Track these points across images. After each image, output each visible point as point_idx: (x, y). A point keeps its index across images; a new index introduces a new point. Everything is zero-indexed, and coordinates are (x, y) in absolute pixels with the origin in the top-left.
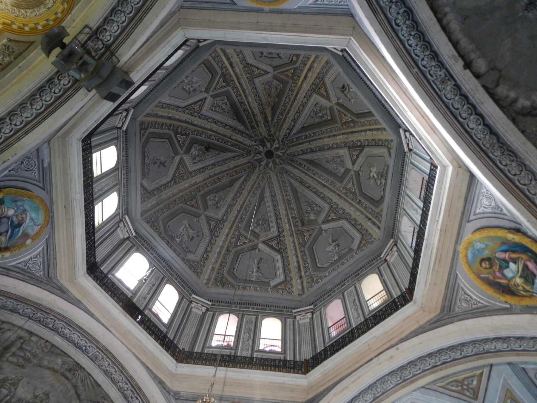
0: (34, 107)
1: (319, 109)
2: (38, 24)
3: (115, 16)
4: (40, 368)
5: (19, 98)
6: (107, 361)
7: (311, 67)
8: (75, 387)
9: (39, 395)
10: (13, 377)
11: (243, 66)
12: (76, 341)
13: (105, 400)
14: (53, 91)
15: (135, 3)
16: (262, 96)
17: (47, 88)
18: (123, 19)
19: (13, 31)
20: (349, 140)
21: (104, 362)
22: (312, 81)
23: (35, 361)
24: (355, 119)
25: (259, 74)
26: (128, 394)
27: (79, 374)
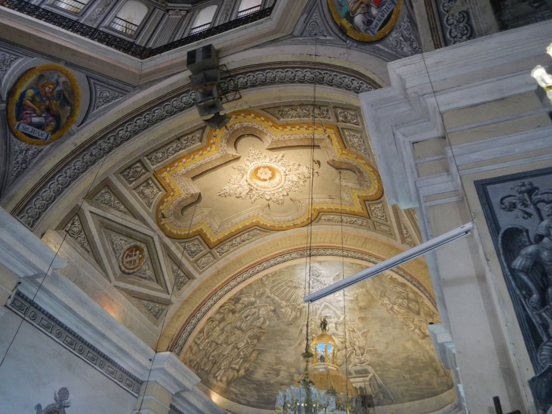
0: (273, 75)
2: (253, 118)
3: (182, 106)
5: (282, 87)
14: (254, 79)
15: (160, 110)
17: (258, 82)
18: (175, 102)
19: (273, 121)
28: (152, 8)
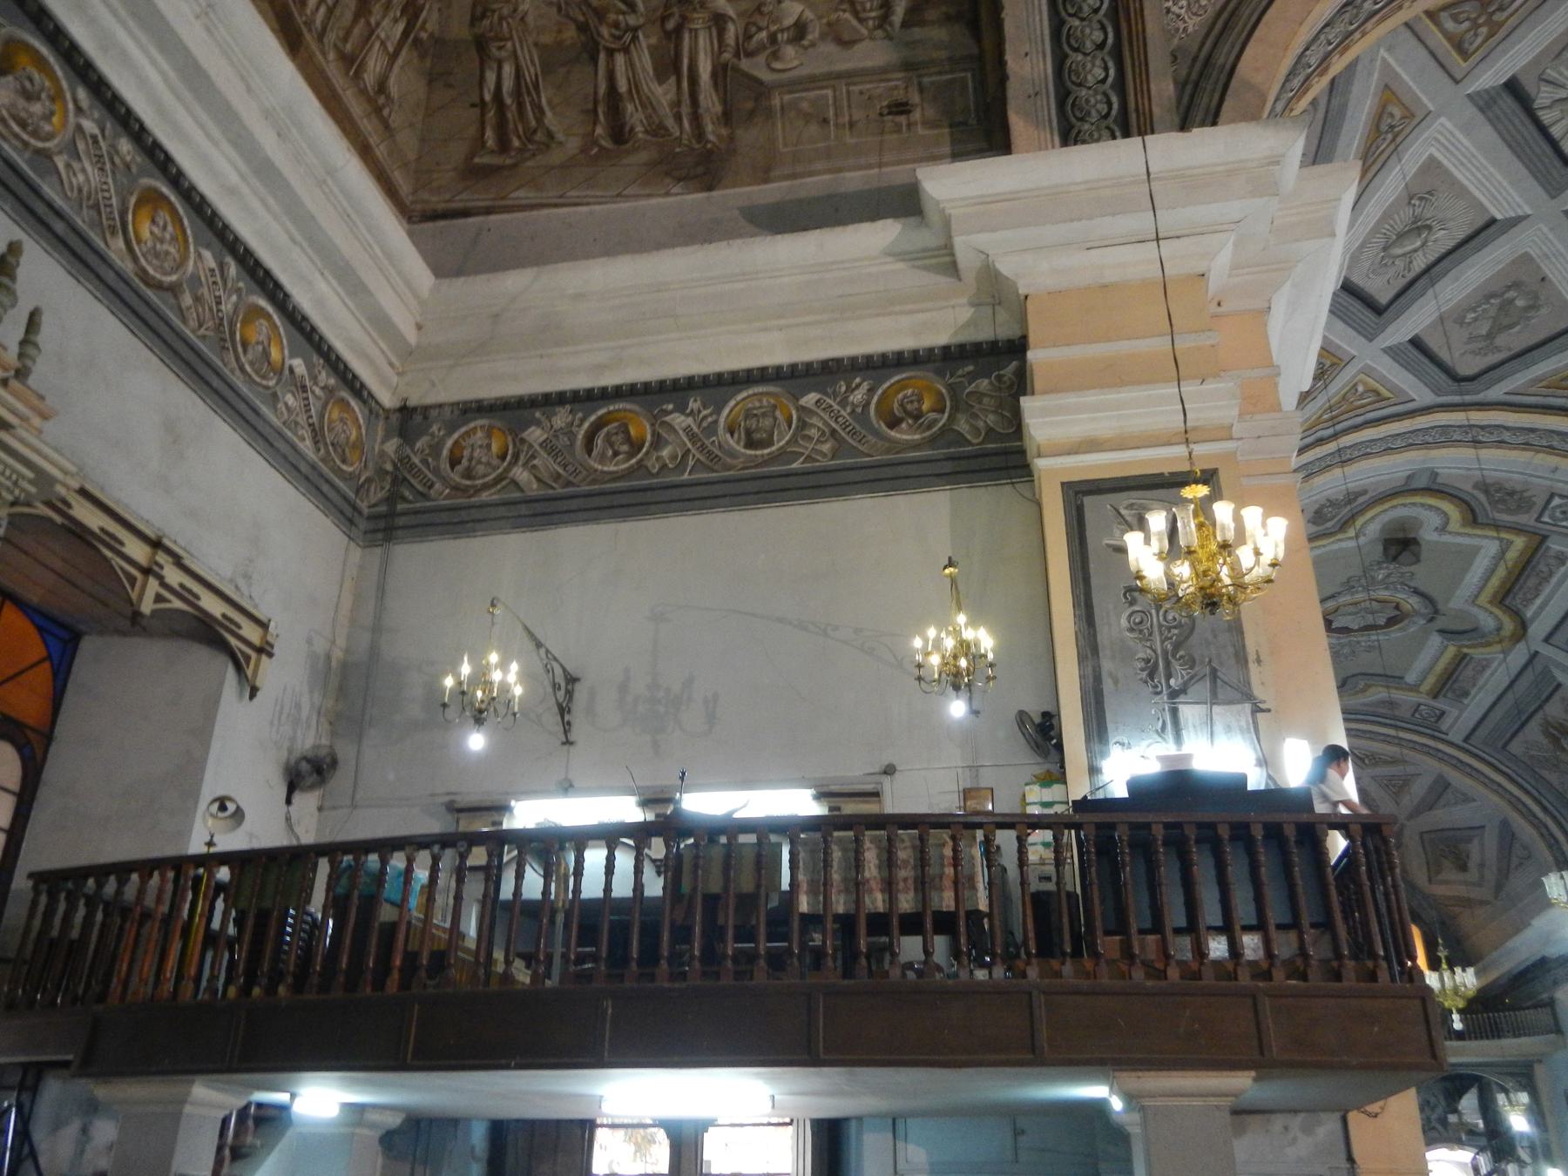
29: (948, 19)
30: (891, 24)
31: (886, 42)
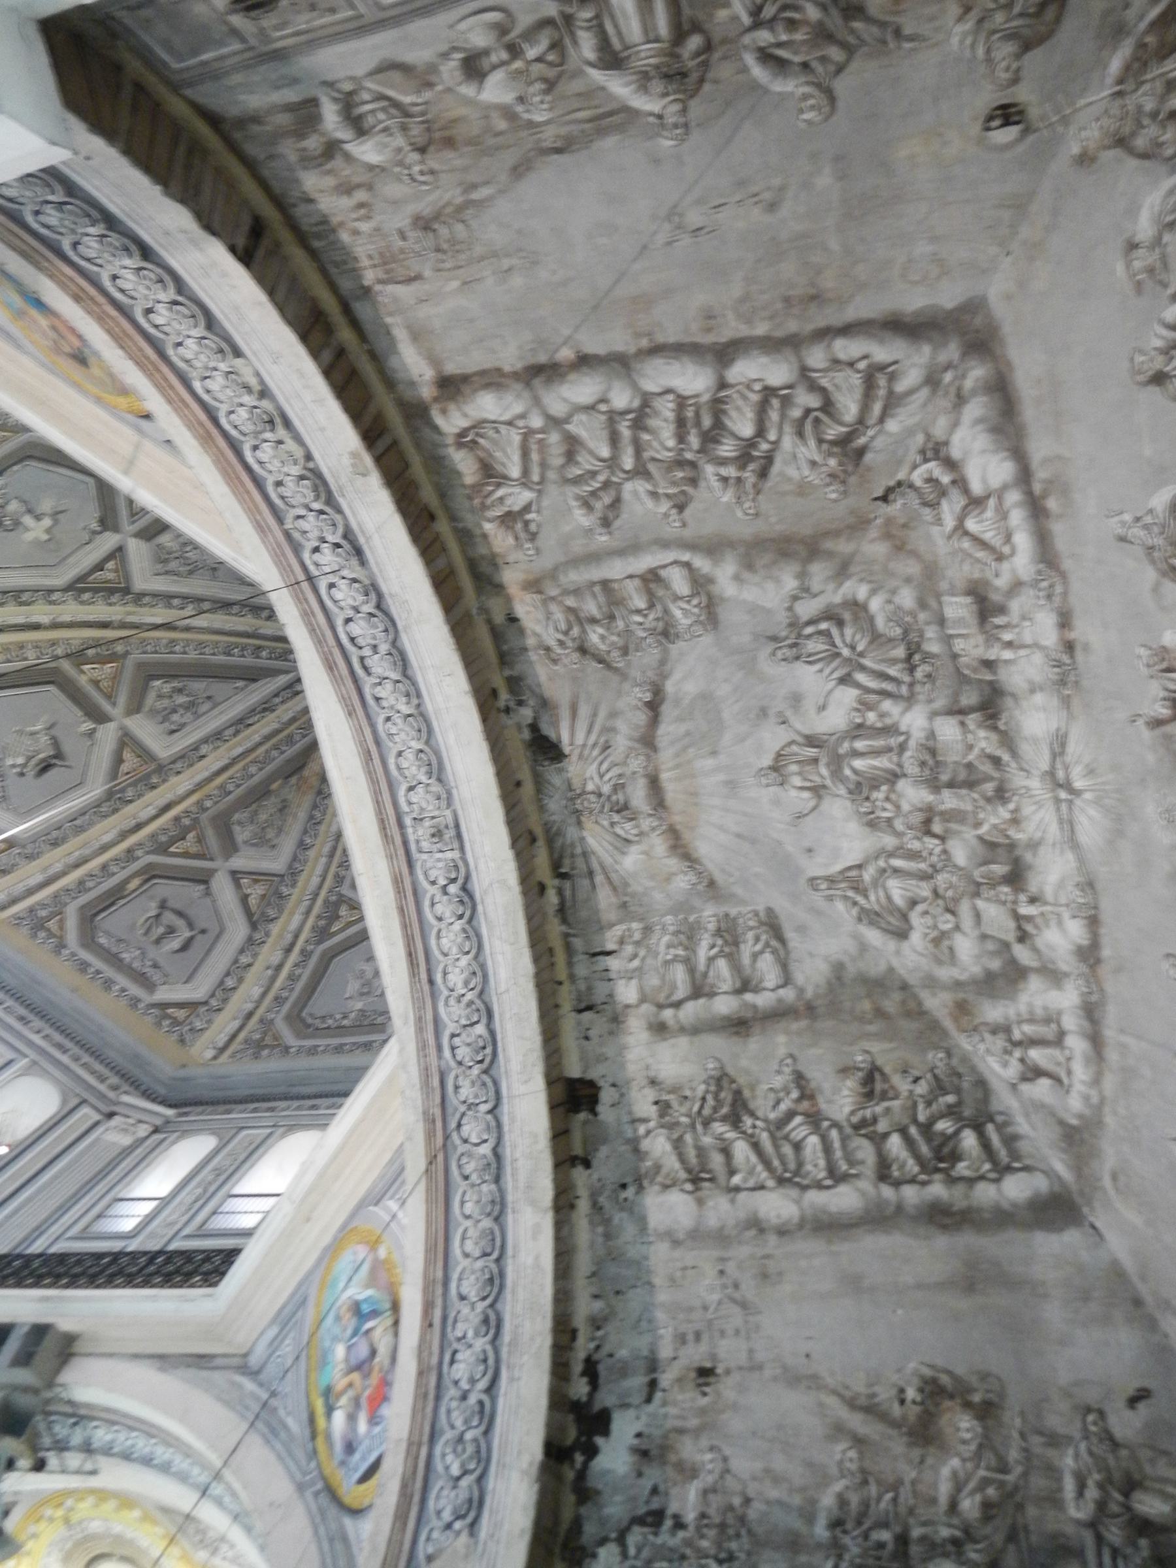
1: (175, 717)
4: (719, 878)
6: (410, 803)
7: (124, 835)
8: (648, 741)
9: (802, 788)
10: (840, 906)
11: (271, 926)
12: (458, 925)
13: (548, 649)
16: (302, 815)
20: (122, 609)
21: (424, 805)
22: (150, 796)
23: (706, 913)
24: (66, 666)
25: (256, 881)
26: (385, 664)
27: (601, 776)
28: (74, 1102)
29: (256, 119)
30: (335, 100)
31: (329, 77)
